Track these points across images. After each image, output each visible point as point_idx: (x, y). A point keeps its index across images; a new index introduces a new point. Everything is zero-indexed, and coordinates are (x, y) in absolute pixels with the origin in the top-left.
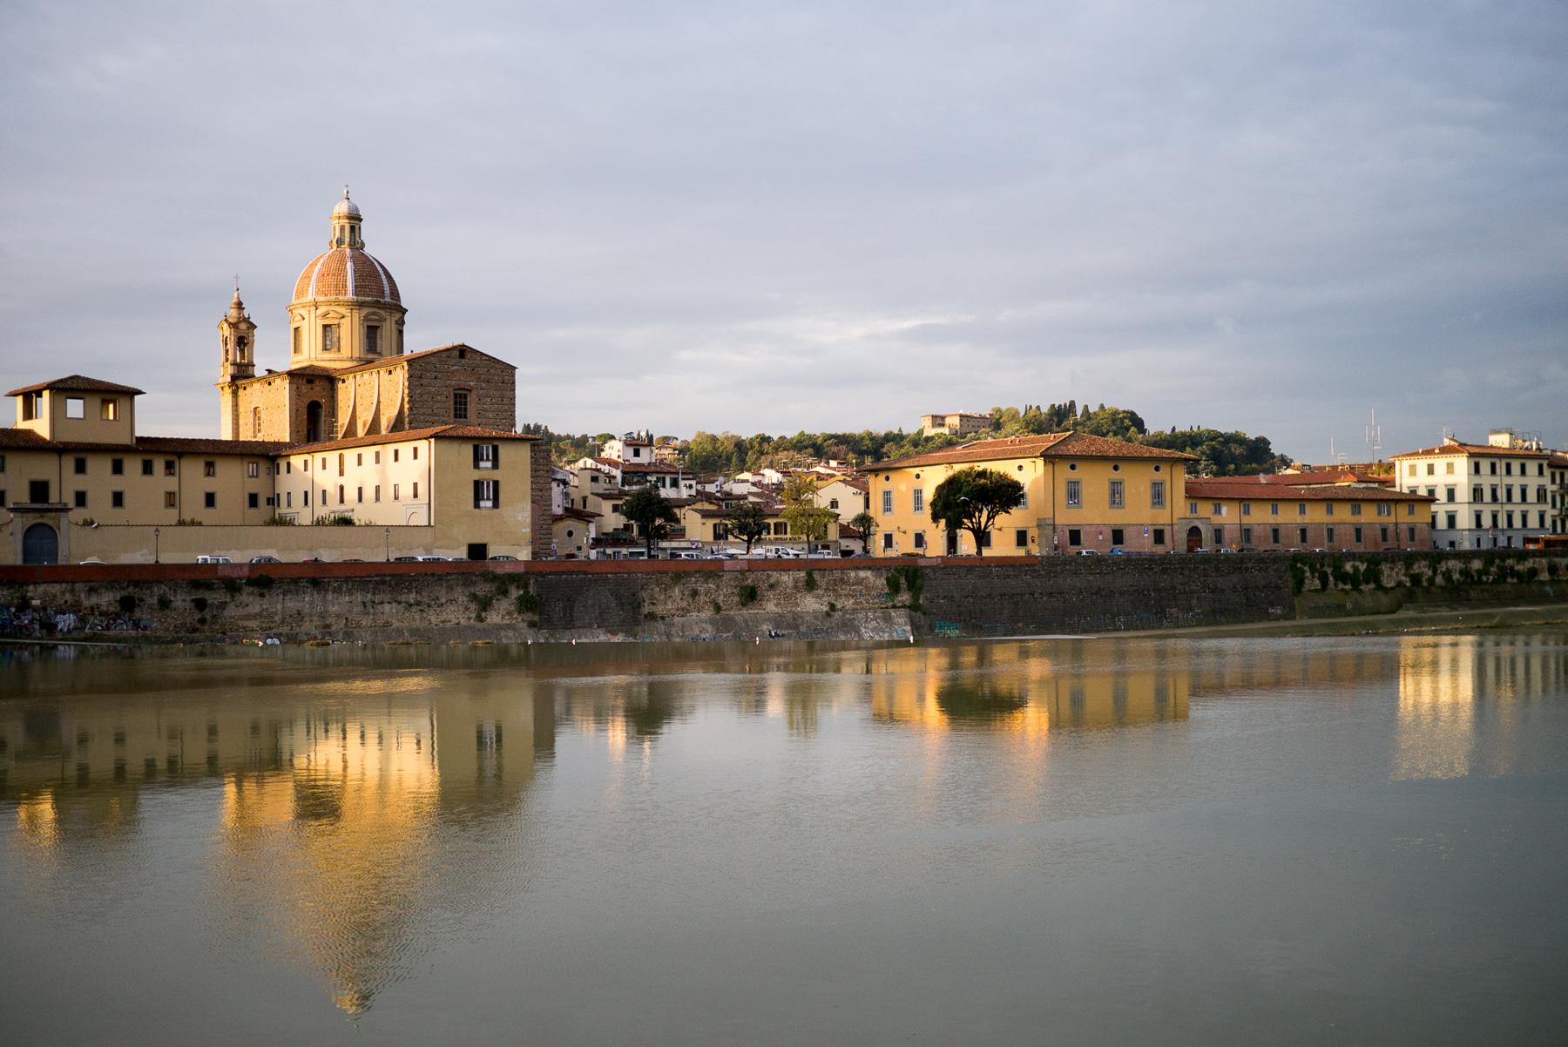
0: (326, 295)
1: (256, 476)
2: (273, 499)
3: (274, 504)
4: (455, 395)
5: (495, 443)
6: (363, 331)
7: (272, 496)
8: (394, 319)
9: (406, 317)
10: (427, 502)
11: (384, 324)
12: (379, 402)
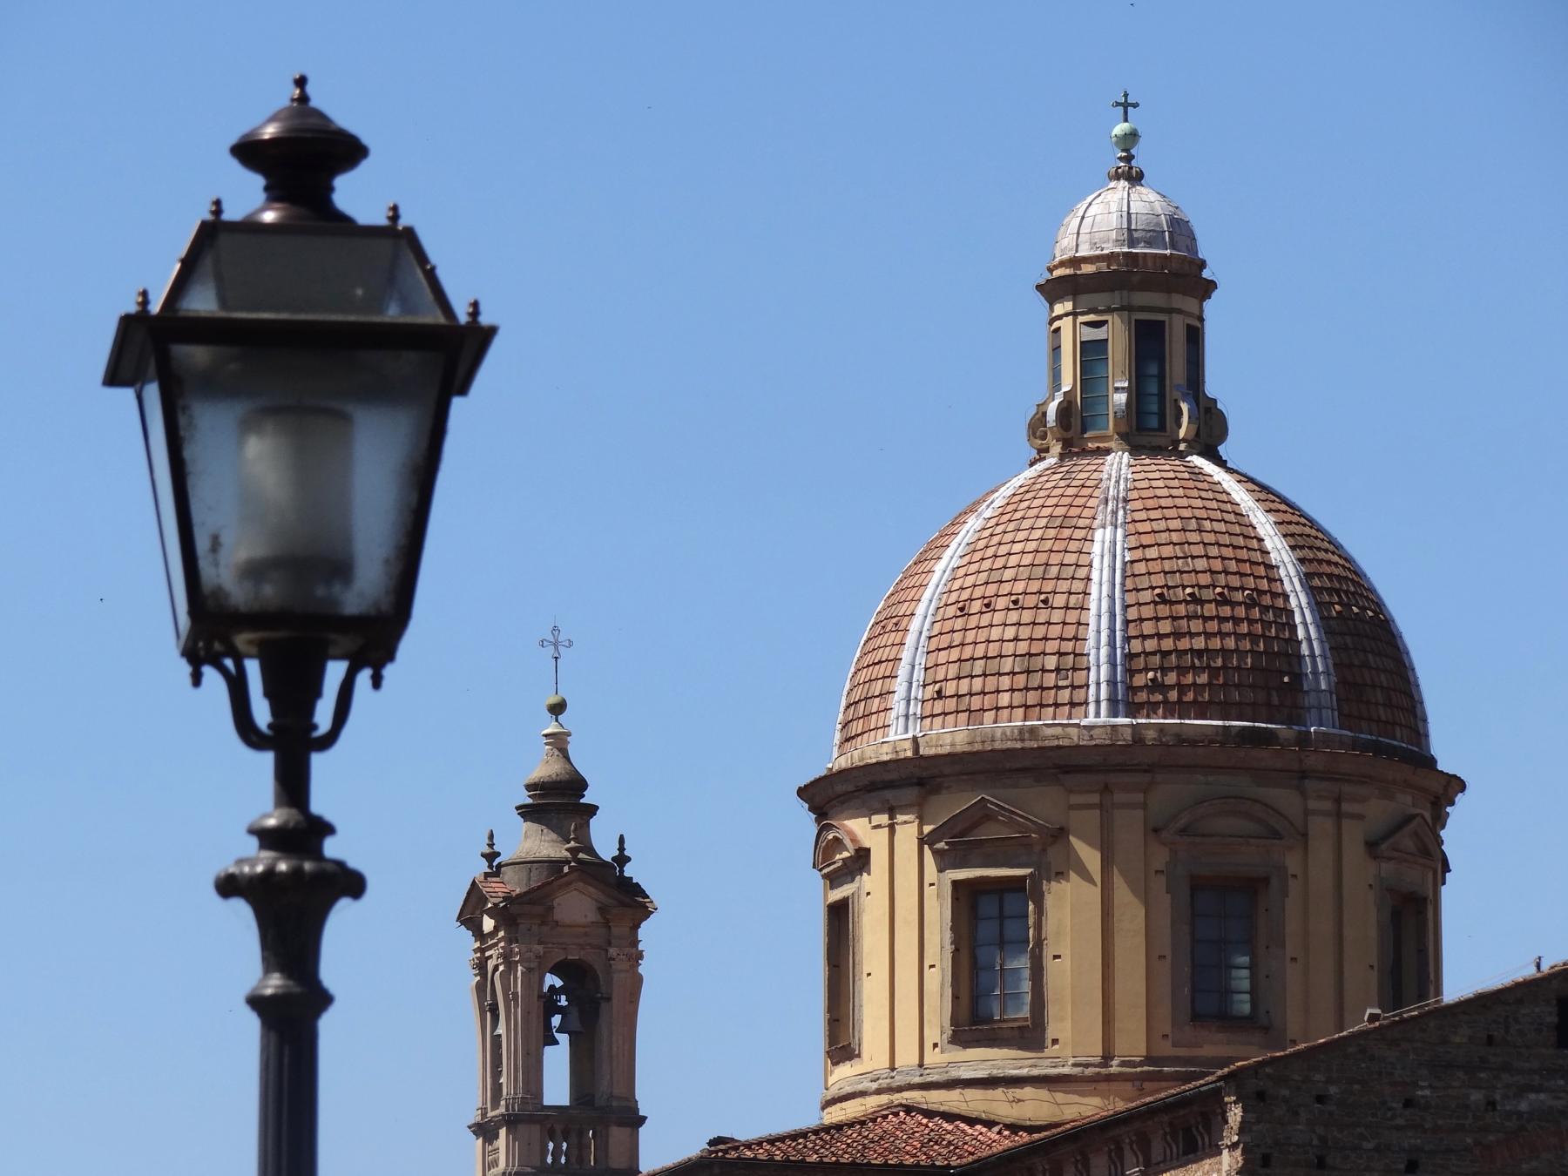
11: (1292, 863)
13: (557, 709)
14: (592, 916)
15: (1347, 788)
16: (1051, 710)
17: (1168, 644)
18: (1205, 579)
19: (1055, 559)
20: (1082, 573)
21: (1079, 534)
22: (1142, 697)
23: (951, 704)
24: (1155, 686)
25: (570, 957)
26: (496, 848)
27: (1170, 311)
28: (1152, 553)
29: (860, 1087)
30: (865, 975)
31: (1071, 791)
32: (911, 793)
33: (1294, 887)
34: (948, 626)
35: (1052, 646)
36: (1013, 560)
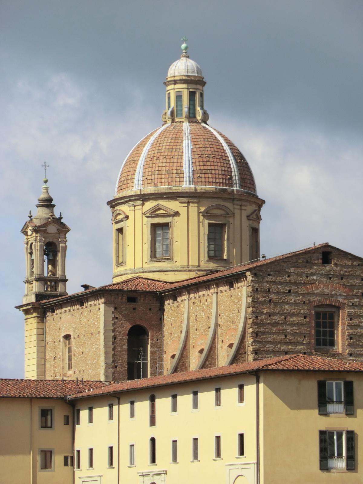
0: (156, 184)
1: (51, 427)
2: (72, 458)
3: (72, 465)
4: (318, 315)
5: (349, 379)
6: (205, 230)
7: (70, 455)
8: (244, 214)
9: (264, 212)
10: (255, 461)
11: (231, 220)
12: (217, 325)
13: (46, 182)
14: (56, 231)
15: (243, 203)
16: (175, 183)
17: (202, 168)
18: (210, 153)
19: (174, 147)
20: (181, 151)
21: (180, 141)
22: (196, 180)
23: (150, 181)
24: (200, 177)
25: (50, 241)
26: (32, 215)
27: (197, 89)
28: (197, 146)
29: (126, 272)
32: (140, 202)
35: (174, 168)
36: (164, 147)
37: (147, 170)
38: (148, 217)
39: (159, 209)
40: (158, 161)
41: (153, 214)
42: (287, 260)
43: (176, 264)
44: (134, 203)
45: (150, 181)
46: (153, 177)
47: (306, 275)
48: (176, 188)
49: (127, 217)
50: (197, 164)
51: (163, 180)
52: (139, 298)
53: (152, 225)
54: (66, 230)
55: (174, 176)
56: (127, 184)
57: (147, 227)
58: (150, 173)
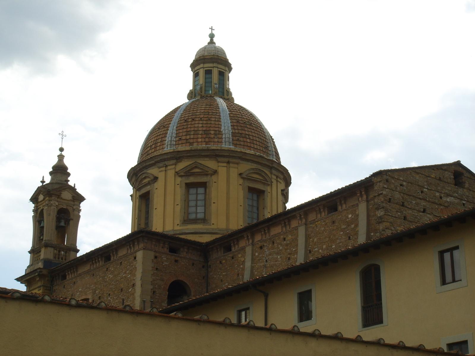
0: (191, 144)
16: (213, 143)
19: (210, 111)
22: (235, 142)
23: (185, 141)
30: (154, 209)
31: (218, 162)
32: (174, 162)
33: (269, 195)
34: (182, 124)
37: (181, 131)
38: (181, 176)
39: (196, 167)
40: (193, 123)
41: (187, 173)
42: (419, 172)
43: (213, 227)
44: (166, 163)
45: (185, 141)
46: (188, 137)
47: (439, 195)
48: (213, 147)
49: (156, 179)
50: (236, 127)
51: (200, 140)
52: (182, 249)
53: (186, 184)
54: (81, 199)
55: (212, 136)
56: (155, 147)
57: (180, 187)
58: (184, 134)
